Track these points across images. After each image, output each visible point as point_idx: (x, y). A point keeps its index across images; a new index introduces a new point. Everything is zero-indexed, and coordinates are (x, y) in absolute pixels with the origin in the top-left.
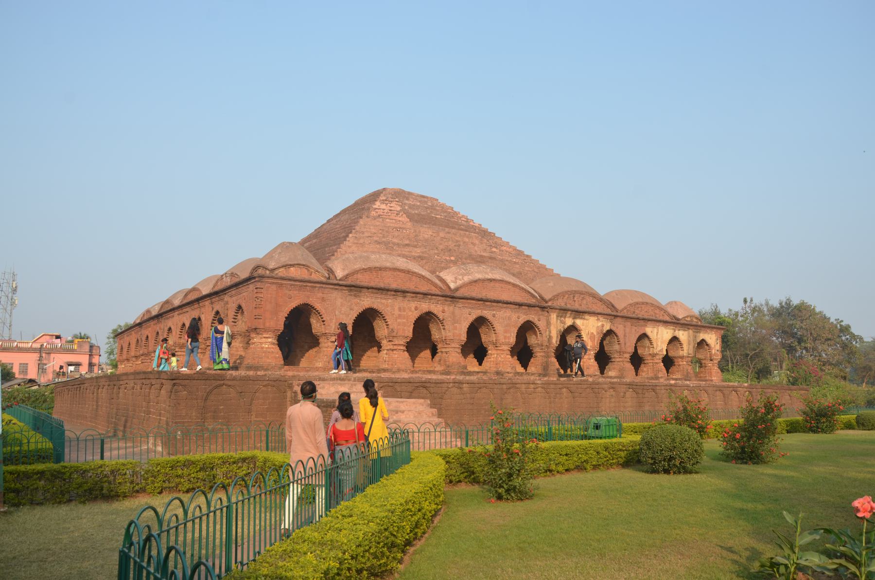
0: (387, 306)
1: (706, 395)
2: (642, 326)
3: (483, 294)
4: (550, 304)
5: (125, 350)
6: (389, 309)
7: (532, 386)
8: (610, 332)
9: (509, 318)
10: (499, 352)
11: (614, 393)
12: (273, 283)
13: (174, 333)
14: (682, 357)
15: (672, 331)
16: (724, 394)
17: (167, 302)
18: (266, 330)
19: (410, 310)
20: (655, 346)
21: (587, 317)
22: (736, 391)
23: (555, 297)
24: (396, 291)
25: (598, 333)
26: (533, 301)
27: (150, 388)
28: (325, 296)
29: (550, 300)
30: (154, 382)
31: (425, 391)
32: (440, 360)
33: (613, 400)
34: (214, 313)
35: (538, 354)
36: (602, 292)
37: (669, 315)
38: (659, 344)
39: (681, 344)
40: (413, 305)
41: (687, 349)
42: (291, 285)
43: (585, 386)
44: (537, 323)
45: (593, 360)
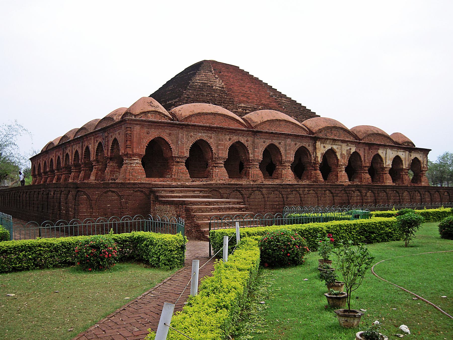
0: (211, 138)
1: (419, 195)
2: (376, 149)
3: (273, 130)
5: (37, 169)
6: (212, 140)
7: (307, 189)
8: (355, 153)
9: (290, 145)
11: (359, 194)
12: (137, 124)
13: (70, 158)
15: (396, 152)
16: (430, 193)
17: (65, 137)
18: (134, 155)
19: (226, 140)
20: (384, 162)
21: (340, 143)
22: (438, 192)
23: (320, 131)
24: (217, 128)
25: (347, 154)
26: (304, 134)
27: (61, 194)
28: (171, 132)
29: (316, 133)
30: (63, 189)
31: (238, 193)
32: (246, 173)
33: (359, 198)
34: (97, 144)
35: (309, 168)
36: (349, 127)
38: (387, 161)
39: (402, 161)
41: (405, 165)
42: (149, 125)
43: (341, 189)
44: (308, 148)
45: (344, 172)
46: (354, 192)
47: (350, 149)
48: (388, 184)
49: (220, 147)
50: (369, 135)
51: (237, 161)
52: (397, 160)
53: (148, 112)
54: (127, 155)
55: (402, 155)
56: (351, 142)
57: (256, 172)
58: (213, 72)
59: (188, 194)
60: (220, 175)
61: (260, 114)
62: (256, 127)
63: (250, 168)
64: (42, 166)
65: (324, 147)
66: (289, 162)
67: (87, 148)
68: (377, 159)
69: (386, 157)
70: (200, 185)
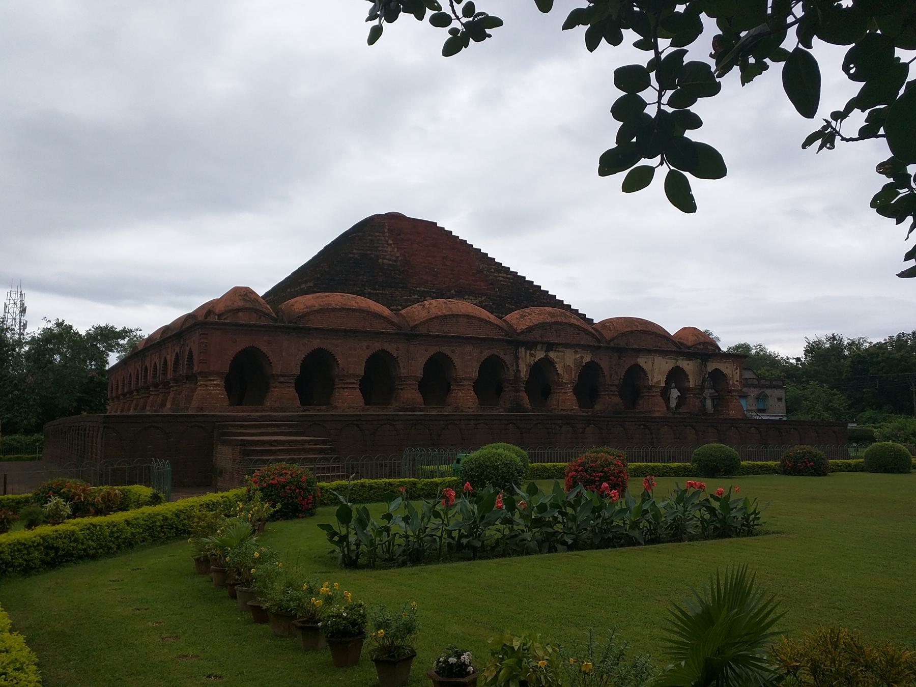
4: (521, 338)
7: (473, 422)
8: (591, 364)
10: (460, 388)
14: (689, 389)
23: (530, 329)
24: (346, 331)
29: (522, 332)
37: (674, 343)
38: (655, 375)
39: (687, 375)
40: (365, 344)
46: (561, 427)
47: (582, 358)
48: (657, 415)
49: (352, 359)
50: (623, 334)
51: (378, 378)
52: (676, 376)
53: (238, 310)
54: (200, 373)
55: (688, 366)
56: (585, 347)
57: (411, 394)
58: (387, 234)
59: (270, 430)
60: (348, 400)
61: (427, 306)
62: (416, 326)
63: (402, 389)
64: (120, 384)
65: (531, 355)
66: (469, 379)
67: (165, 358)
68: (636, 372)
69: (653, 370)
70: (292, 416)
